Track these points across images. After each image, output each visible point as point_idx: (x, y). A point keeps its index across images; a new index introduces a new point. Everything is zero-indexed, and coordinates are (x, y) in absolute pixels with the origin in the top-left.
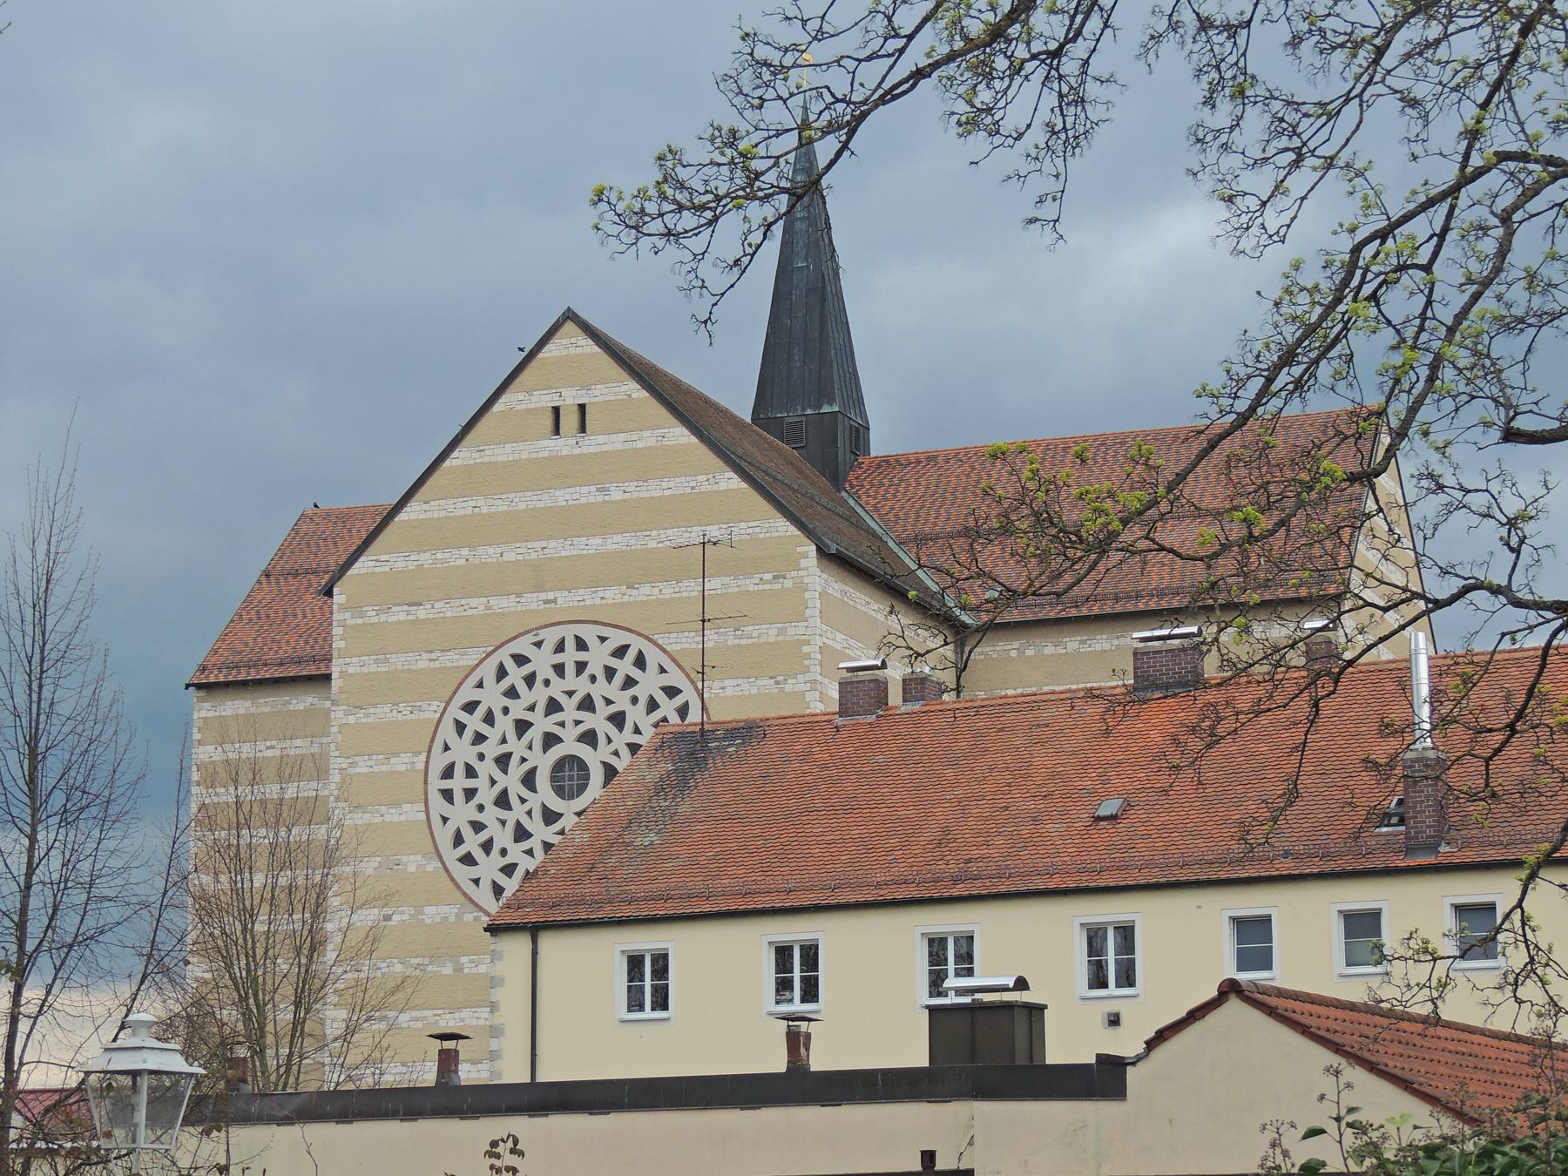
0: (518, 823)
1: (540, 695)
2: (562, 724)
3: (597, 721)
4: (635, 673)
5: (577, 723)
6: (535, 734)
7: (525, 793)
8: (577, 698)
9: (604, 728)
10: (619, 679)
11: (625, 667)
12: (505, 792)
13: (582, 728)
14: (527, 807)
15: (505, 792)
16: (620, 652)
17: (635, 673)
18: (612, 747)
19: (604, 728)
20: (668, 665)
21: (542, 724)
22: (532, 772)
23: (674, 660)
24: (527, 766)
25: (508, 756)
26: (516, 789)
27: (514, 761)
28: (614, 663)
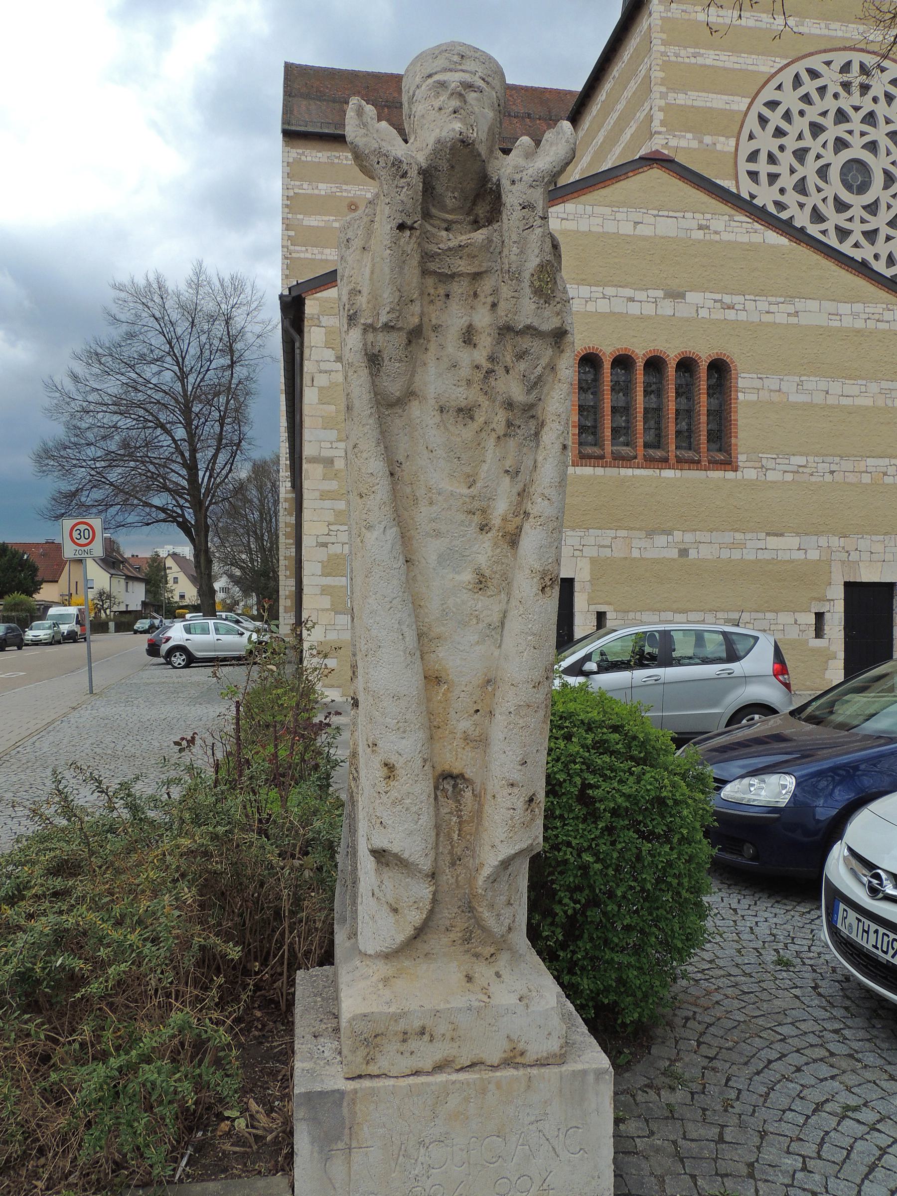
0: (864, 233)
1: (786, 159)
2: (818, 157)
3: (833, 131)
4: (819, 82)
5: (824, 145)
6: (813, 180)
7: (848, 214)
8: (807, 134)
9: (840, 130)
10: (815, 96)
11: (810, 86)
12: (838, 228)
13: (830, 145)
14: (857, 220)
15: (838, 228)
16: (797, 82)
17: (819, 82)
18: (857, 134)
19: (840, 130)
20: (827, 57)
21: (809, 169)
22: (836, 199)
23: (825, 51)
24: (830, 201)
25: (815, 209)
26: (840, 219)
27: (821, 207)
28: (802, 91)
